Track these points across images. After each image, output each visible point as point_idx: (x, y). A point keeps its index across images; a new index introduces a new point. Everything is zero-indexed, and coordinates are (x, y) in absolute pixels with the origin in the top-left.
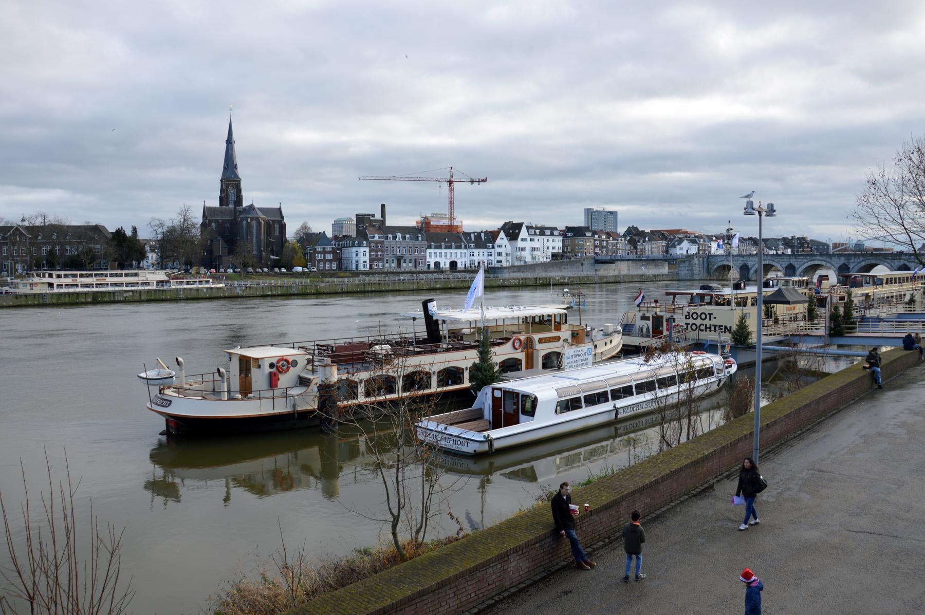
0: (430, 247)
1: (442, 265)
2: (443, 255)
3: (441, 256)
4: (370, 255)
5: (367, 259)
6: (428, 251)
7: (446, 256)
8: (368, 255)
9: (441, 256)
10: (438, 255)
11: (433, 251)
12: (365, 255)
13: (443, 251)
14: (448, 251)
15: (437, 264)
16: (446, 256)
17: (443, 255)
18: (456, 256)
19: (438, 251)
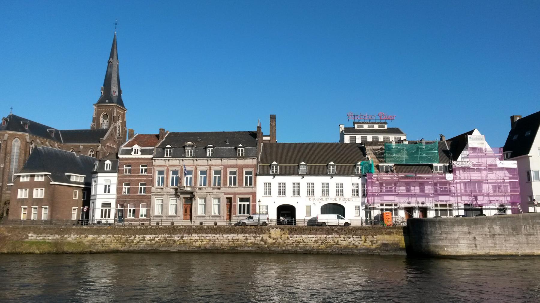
0: (265, 172)
1: (301, 216)
2: (304, 190)
3: (297, 193)
4: (119, 191)
5: (112, 198)
6: (261, 180)
7: (311, 192)
8: (114, 189)
9: (297, 193)
10: (289, 190)
11: (276, 181)
12: (107, 189)
13: (304, 181)
14: (318, 181)
15: (286, 212)
16: (311, 192)
17: (304, 190)
18: (340, 192)
19: (289, 180)
